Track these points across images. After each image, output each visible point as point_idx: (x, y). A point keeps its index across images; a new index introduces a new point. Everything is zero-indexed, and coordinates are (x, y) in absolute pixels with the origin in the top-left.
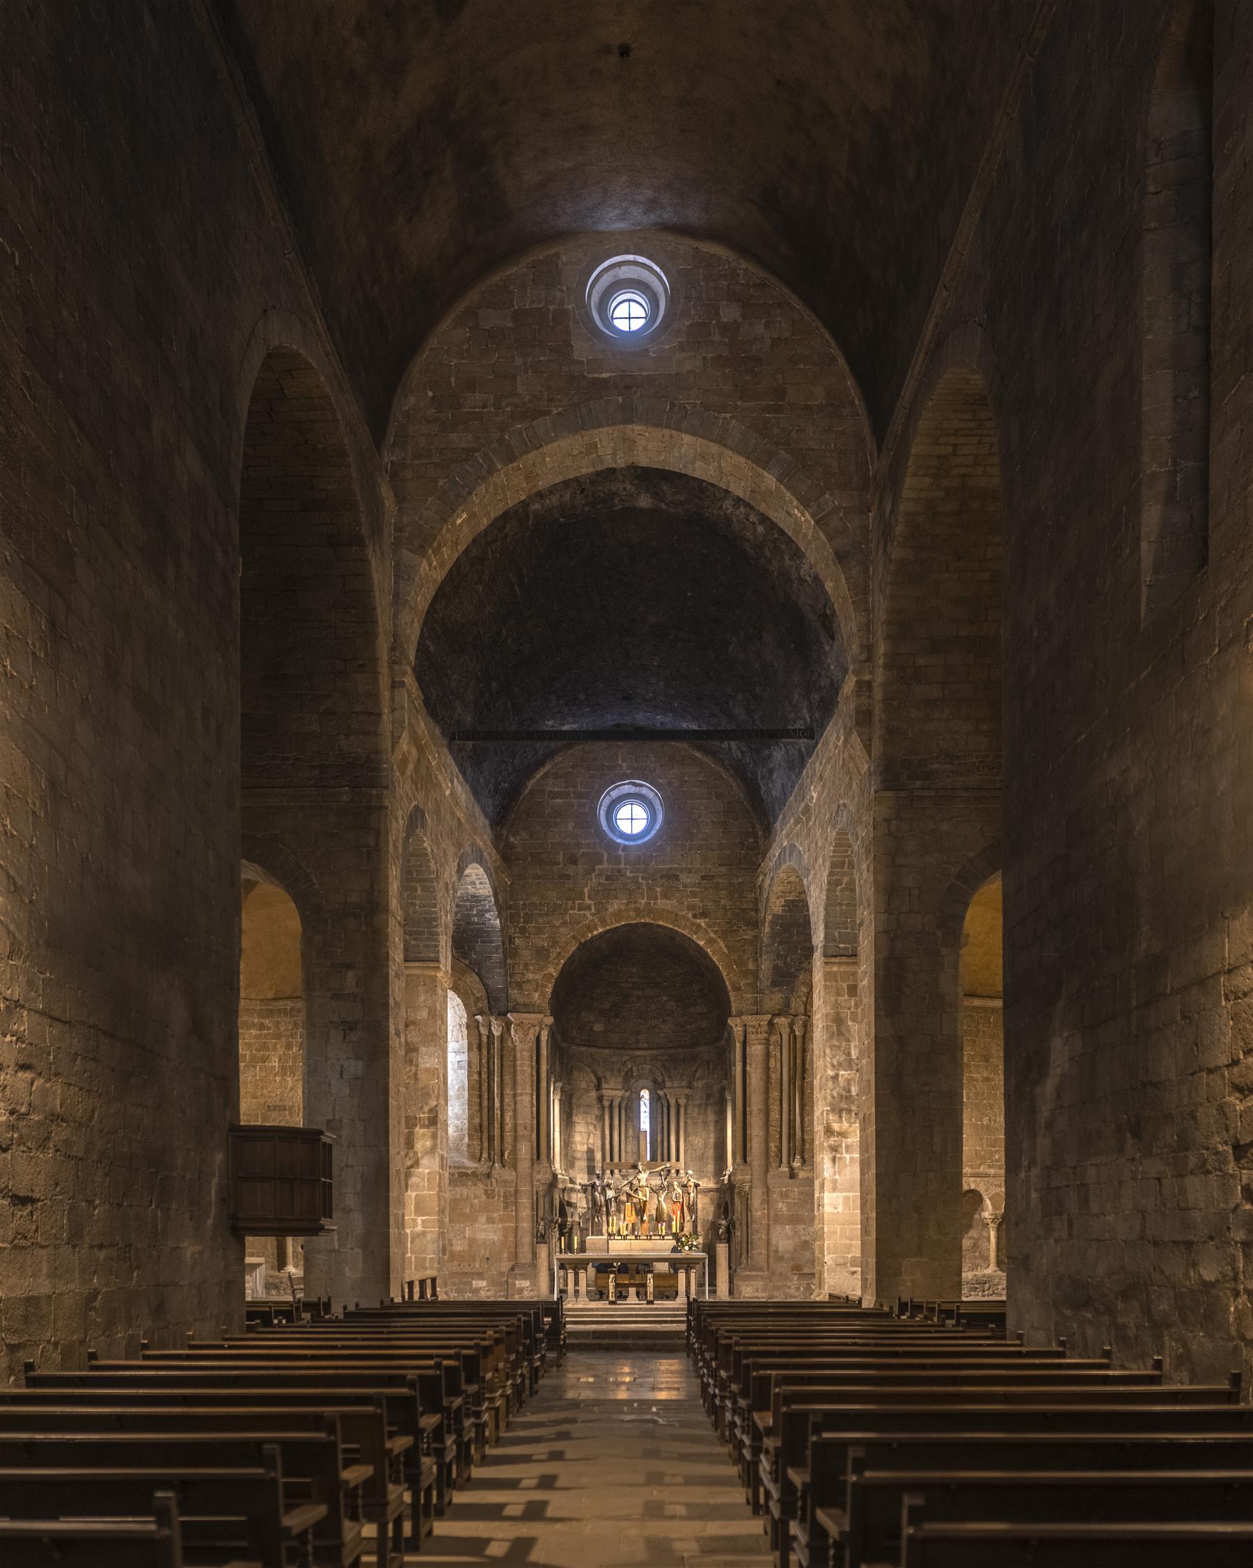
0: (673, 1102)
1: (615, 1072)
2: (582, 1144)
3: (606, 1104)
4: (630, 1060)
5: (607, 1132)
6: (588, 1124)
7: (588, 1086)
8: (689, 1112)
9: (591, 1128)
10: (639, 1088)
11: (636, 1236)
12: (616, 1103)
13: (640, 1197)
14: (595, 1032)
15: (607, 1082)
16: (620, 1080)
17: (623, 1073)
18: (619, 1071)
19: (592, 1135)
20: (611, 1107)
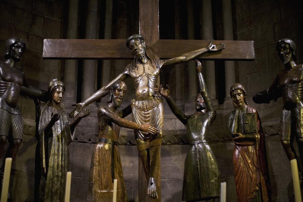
13: (138, 123)
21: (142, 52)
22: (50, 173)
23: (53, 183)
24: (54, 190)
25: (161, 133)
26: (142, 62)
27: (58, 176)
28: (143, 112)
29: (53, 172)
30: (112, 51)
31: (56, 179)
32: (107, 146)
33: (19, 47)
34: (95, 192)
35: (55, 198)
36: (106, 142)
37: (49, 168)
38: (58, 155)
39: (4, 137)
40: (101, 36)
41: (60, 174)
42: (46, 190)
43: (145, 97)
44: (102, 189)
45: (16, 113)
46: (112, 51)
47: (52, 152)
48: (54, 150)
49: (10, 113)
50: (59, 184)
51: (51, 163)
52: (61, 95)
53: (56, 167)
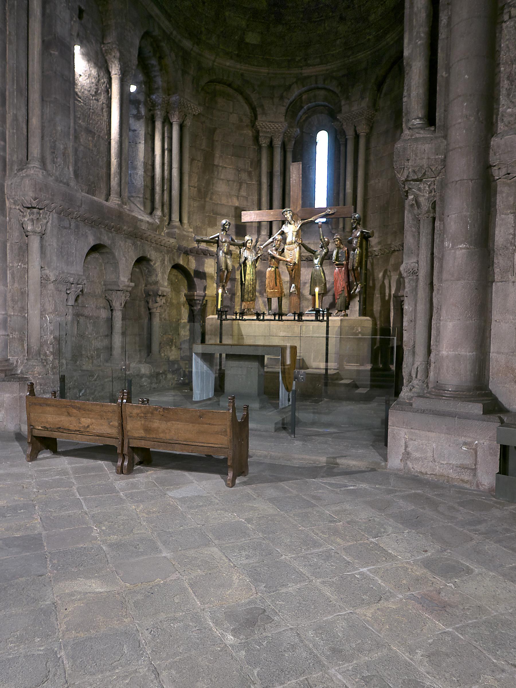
0: (350, 134)
1: (276, 100)
2: (229, 196)
3: (264, 142)
4: (296, 82)
5: (265, 180)
6: (239, 170)
7: (241, 120)
8: (373, 144)
9: (244, 176)
10: (314, 129)
11: (258, 315)
12: (278, 143)
14: (247, 44)
15: (264, 113)
16: (283, 110)
17: (287, 102)
18: (282, 98)
19: (244, 186)
20: (271, 146)
21: (289, 219)
22: (246, 283)
23: (248, 287)
24: (249, 290)
25: (297, 262)
26: (290, 224)
27: (250, 284)
28: (289, 252)
29: (248, 283)
30: (276, 217)
31: (249, 285)
32: (273, 269)
33: (227, 225)
34: (268, 291)
35: (250, 294)
36: (272, 267)
37: (246, 281)
38: (250, 274)
39: (224, 269)
40: (271, 208)
41: (252, 283)
42: (245, 291)
43: (291, 243)
44: (270, 290)
45: (229, 257)
46: (276, 217)
47: (247, 273)
48: (248, 271)
49: (225, 257)
50: (251, 288)
51: (247, 277)
52: (250, 244)
53: (249, 280)
